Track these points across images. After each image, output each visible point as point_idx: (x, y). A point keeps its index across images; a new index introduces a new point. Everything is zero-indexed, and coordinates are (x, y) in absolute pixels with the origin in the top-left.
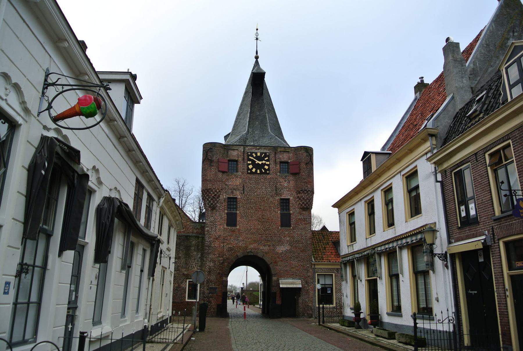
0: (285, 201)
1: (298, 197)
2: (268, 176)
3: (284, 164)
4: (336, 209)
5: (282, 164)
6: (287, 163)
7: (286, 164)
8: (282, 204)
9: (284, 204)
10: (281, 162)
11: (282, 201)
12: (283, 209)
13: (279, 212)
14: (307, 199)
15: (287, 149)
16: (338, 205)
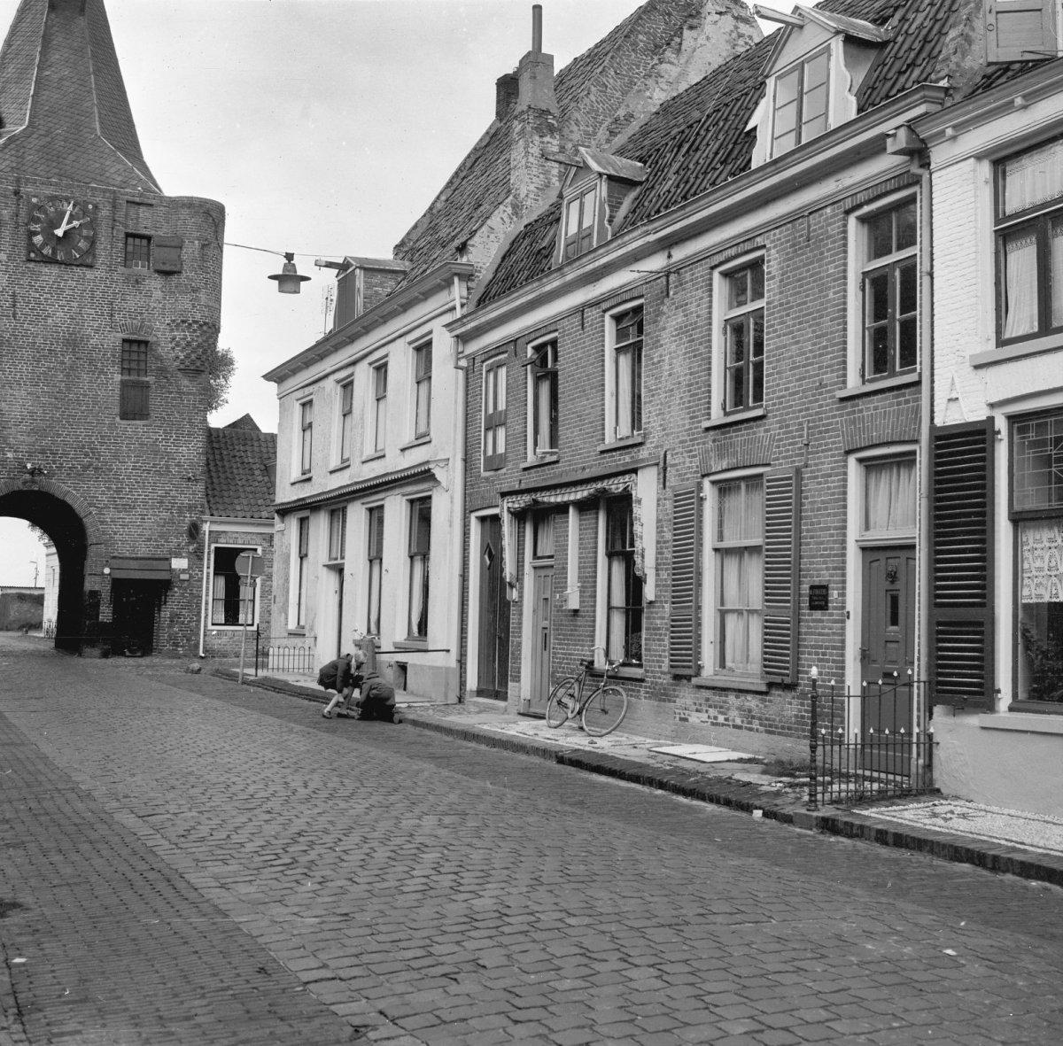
0: (135, 348)
1: (173, 339)
2: (89, 274)
3: (138, 241)
4: (273, 385)
5: (130, 240)
6: (149, 238)
7: (145, 242)
8: (126, 356)
9: (134, 357)
10: (128, 235)
11: (127, 346)
12: (129, 370)
13: (118, 378)
14: (198, 346)
15: (149, 198)
16: (278, 376)
